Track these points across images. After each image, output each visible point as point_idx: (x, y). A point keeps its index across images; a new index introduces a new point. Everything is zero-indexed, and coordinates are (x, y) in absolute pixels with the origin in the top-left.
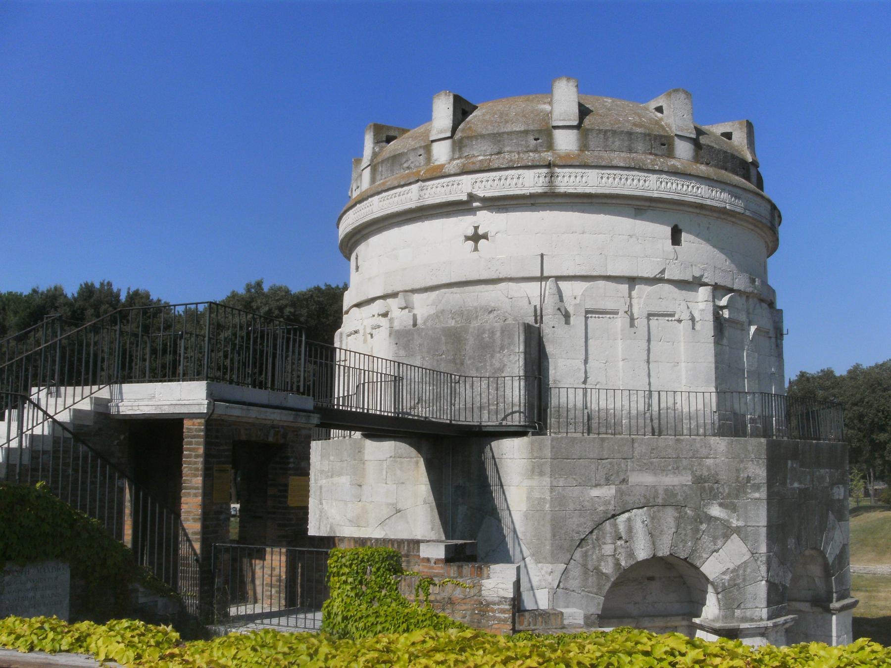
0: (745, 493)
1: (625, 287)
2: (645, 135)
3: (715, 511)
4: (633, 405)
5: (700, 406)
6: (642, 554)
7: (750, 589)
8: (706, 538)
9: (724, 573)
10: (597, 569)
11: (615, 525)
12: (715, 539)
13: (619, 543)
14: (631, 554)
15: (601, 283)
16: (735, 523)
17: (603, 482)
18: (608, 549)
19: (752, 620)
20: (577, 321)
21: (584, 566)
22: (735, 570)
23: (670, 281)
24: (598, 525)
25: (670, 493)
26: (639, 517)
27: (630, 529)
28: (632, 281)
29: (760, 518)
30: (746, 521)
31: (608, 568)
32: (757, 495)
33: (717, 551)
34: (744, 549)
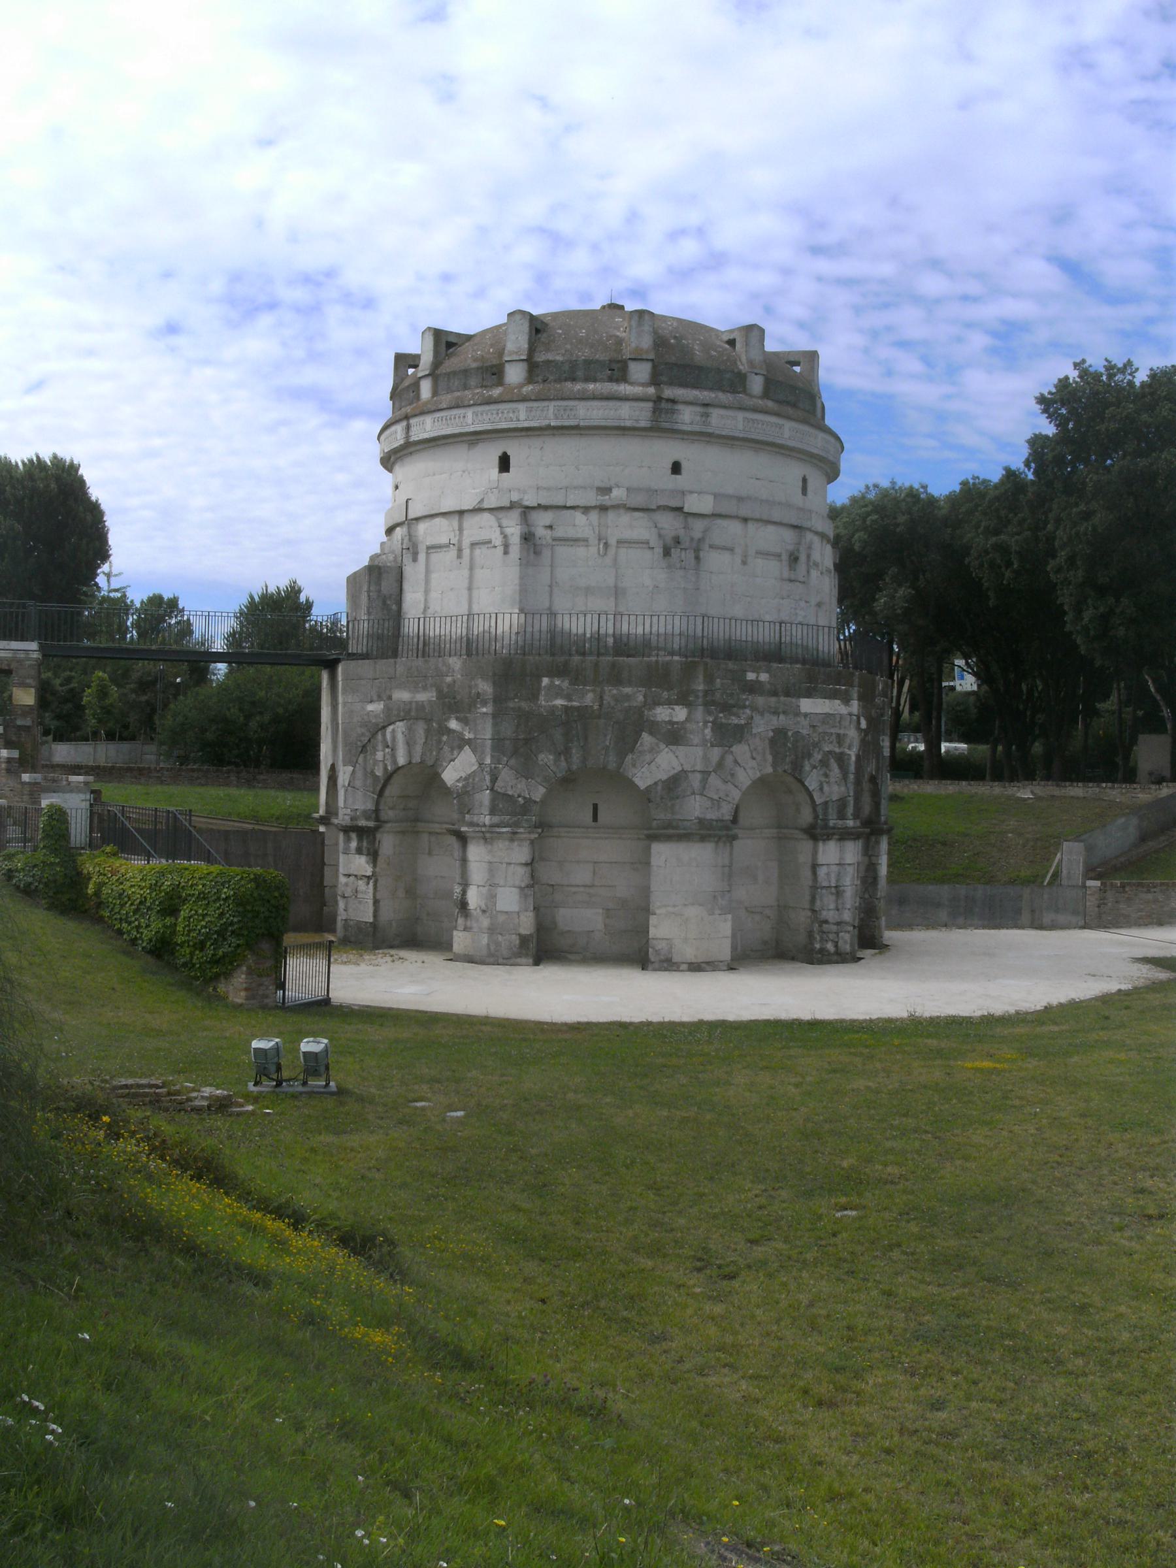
0: (476, 708)
1: (455, 522)
2: (478, 368)
3: (453, 724)
4: (454, 630)
5: (507, 628)
6: (401, 761)
7: (477, 796)
8: (446, 748)
9: (458, 781)
10: (372, 772)
11: (384, 735)
12: (452, 749)
13: (387, 750)
14: (395, 761)
15: (437, 520)
16: (468, 736)
17: (375, 698)
18: (379, 755)
19: (478, 825)
20: (422, 557)
21: (365, 769)
22: (466, 779)
23: (491, 510)
24: (374, 735)
25: (420, 707)
26: (400, 727)
27: (394, 738)
28: (461, 513)
29: (487, 732)
30: (475, 734)
31: (379, 772)
32: (484, 710)
33: (453, 760)
34: (473, 759)
